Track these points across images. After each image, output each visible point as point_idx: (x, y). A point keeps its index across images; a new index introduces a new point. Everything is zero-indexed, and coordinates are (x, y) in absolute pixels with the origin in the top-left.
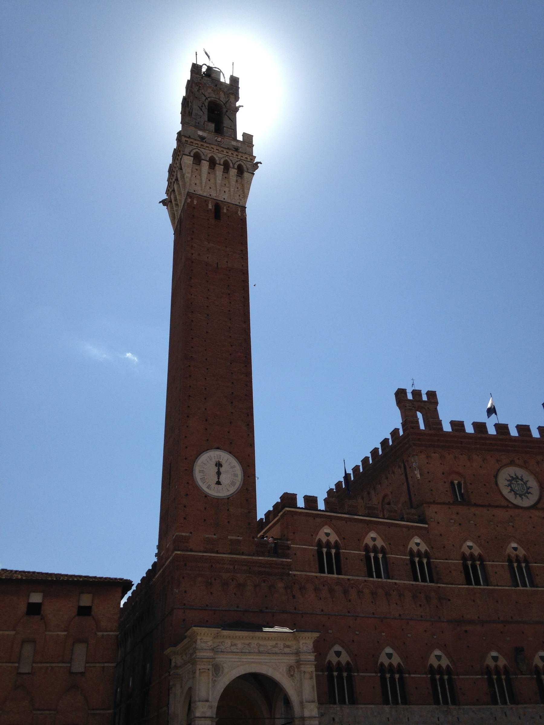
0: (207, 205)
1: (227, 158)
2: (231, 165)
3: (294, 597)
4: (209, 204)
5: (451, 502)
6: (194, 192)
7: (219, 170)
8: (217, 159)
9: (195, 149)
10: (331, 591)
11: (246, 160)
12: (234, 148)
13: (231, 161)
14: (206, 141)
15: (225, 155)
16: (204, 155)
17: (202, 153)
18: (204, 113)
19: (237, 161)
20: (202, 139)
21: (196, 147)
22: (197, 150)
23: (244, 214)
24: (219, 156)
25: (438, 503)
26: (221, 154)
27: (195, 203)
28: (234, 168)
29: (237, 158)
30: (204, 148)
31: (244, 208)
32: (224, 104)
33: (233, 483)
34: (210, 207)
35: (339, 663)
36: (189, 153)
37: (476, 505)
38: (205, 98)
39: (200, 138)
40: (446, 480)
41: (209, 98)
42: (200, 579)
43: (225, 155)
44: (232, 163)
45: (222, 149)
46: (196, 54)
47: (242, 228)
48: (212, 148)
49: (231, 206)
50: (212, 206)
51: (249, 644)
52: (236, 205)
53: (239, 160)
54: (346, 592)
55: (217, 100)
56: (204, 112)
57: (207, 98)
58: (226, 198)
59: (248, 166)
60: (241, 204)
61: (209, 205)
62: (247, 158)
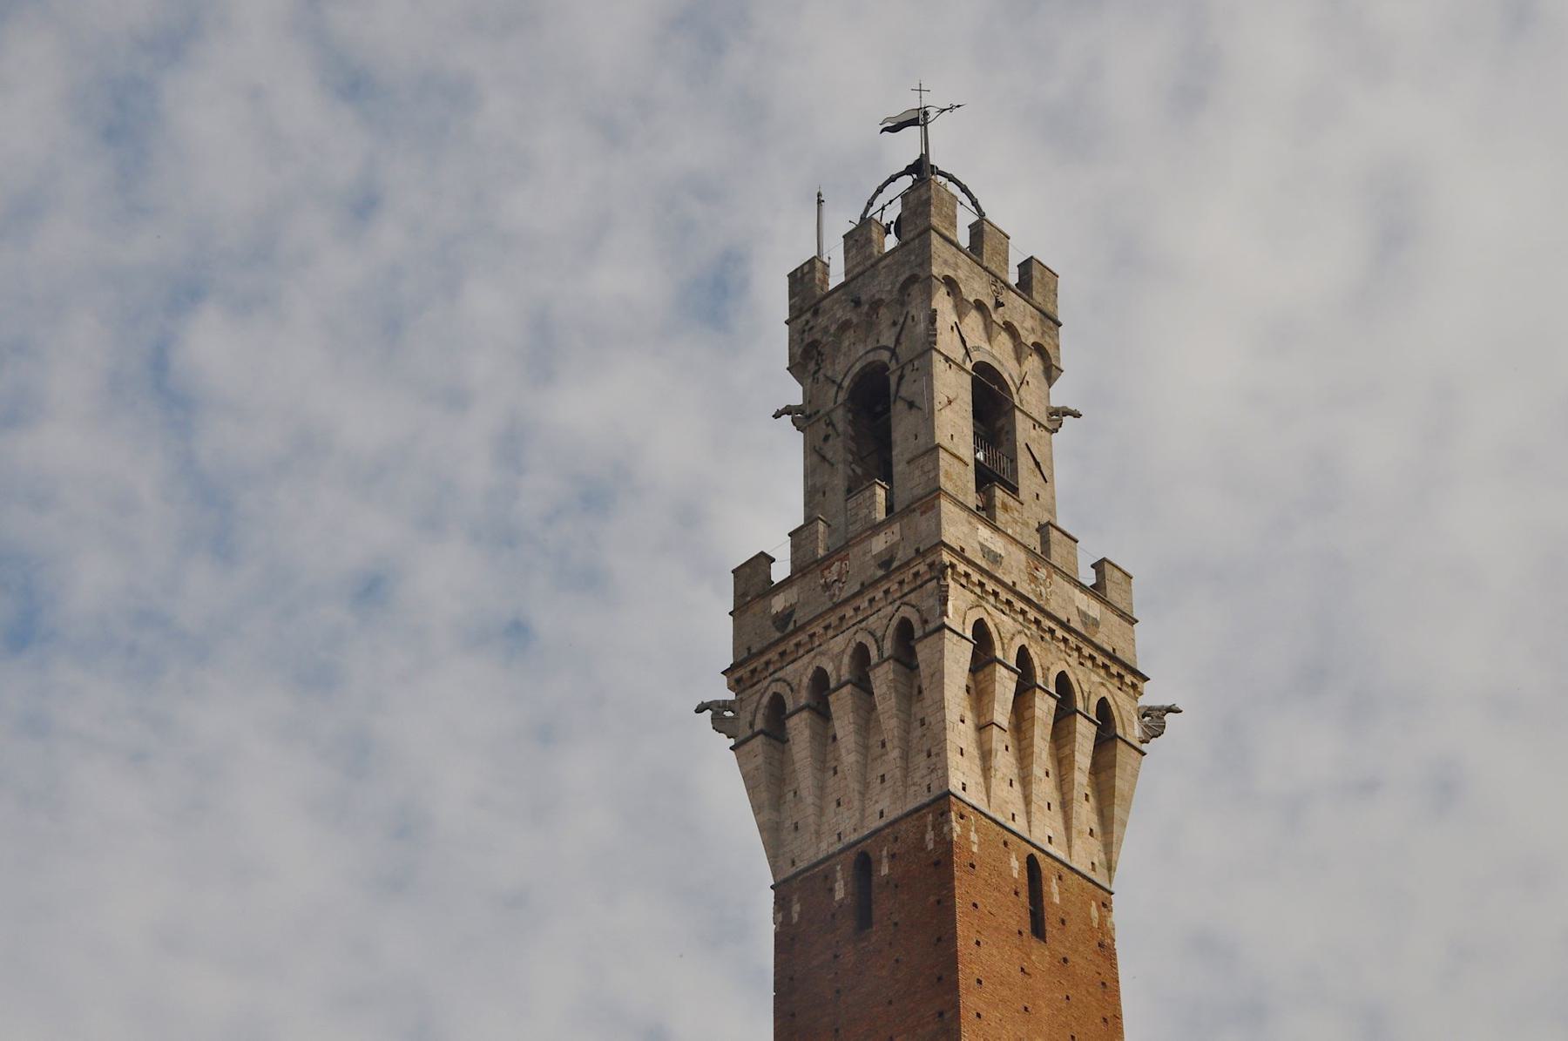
0: (832, 890)
1: (860, 637)
2: (874, 653)
4: (836, 881)
6: (793, 871)
7: (843, 704)
8: (829, 668)
9: (767, 688)
11: (919, 582)
12: (881, 566)
13: (872, 634)
14: (795, 621)
15: (854, 625)
16: (792, 690)
17: (789, 684)
18: (832, 465)
19: (890, 620)
20: (783, 619)
21: (770, 679)
22: (777, 688)
23: (946, 829)
24: (837, 650)
26: (842, 632)
27: (796, 917)
28: (882, 661)
29: (891, 603)
30: (791, 658)
31: (942, 802)
32: (893, 353)
34: (839, 894)
36: (751, 725)
38: (835, 388)
39: (778, 629)
41: (845, 376)
43: (854, 625)
44: (876, 641)
45: (839, 613)
46: (820, 202)
47: (939, 902)
48: (812, 636)
49: (903, 826)
50: (845, 885)
52: (917, 810)
53: (898, 603)
55: (871, 357)
56: (832, 461)
58: (884, 804)
59: (925, 606)
60: (936, 792)
61: (837, 885)
62: (916, 575)
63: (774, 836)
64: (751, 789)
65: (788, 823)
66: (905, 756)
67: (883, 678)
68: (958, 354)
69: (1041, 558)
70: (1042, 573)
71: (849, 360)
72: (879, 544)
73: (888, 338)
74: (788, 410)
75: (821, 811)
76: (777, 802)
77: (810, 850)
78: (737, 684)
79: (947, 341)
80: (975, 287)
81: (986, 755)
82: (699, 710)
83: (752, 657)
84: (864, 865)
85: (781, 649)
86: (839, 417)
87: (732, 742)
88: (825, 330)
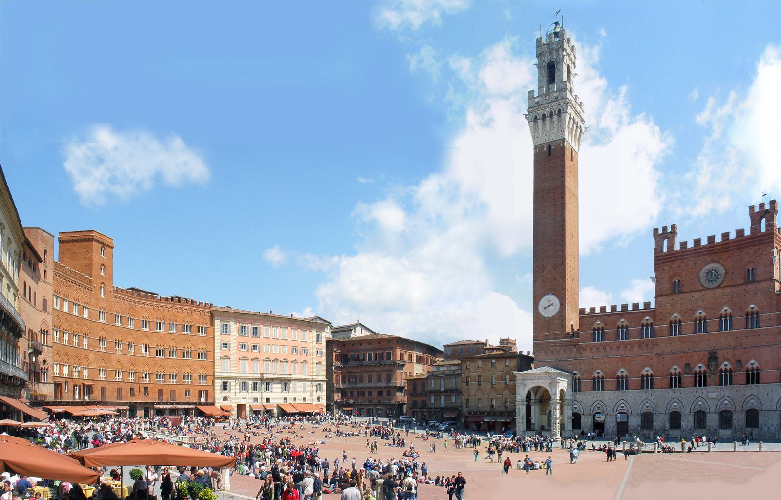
3: (581, 353)
5: (670, 293)
7: (548, 119)
10: (598, 349)
20: (537, 103)
25: (664, 296)
28: (555, 115)
32: (556, 60)
33: (555, 309)
34: (545, 150)
35: (598, 377)
37: (684, 293)
40: (670, 281)
42: (543, 351)
51: (535, 377)
54: (604, 348)
57: (545, 63)
59: (564, 107)
63: (534, 137)
64: (531, 130)
65: (536, 137)
66: (558, 130)
67: (555, 117)
68: (566, 63)
69: (576, 101)
70: (576, 104)
71: (547, 59)
72: (555, 95)
73: (555, 57)
74: (536, 64)
75: (542, 136)
76: (535, 132)
77: (540, 142)
78: (529, 112)
79: (565, 61)
80: (568, 51)
81: (568, 133)
82: (523, 115)
83: (531, 108)
84: (549, 146)
85: (537, 108)
86: (545, 68)
87: (528, 121)
88: (543, 52)
